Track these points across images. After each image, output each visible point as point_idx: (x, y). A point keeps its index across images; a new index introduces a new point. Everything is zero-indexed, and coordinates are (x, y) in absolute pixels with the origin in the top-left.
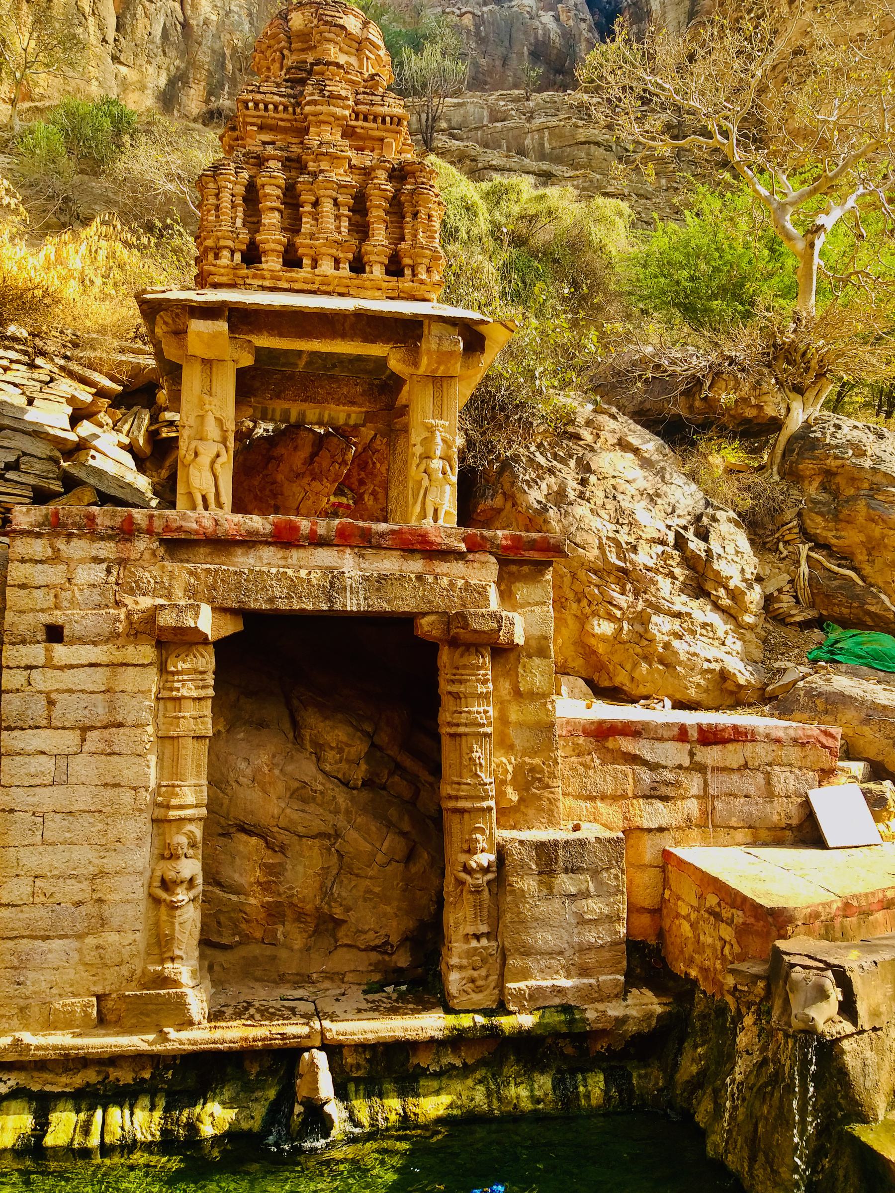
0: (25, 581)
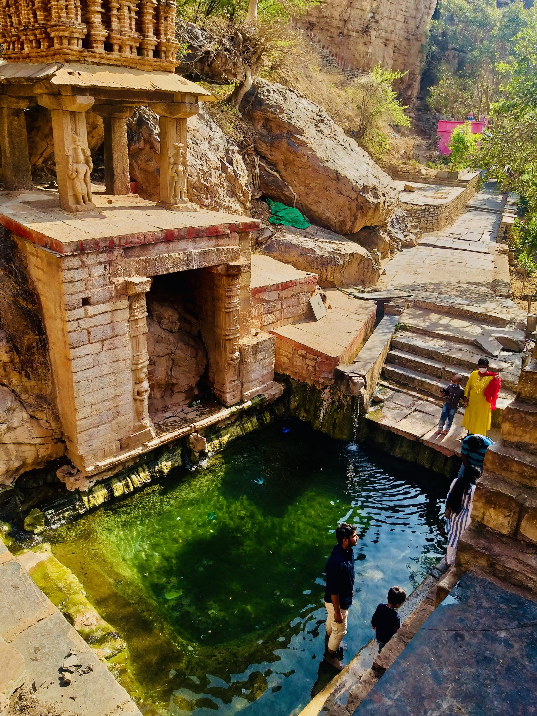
0: (71, 279)
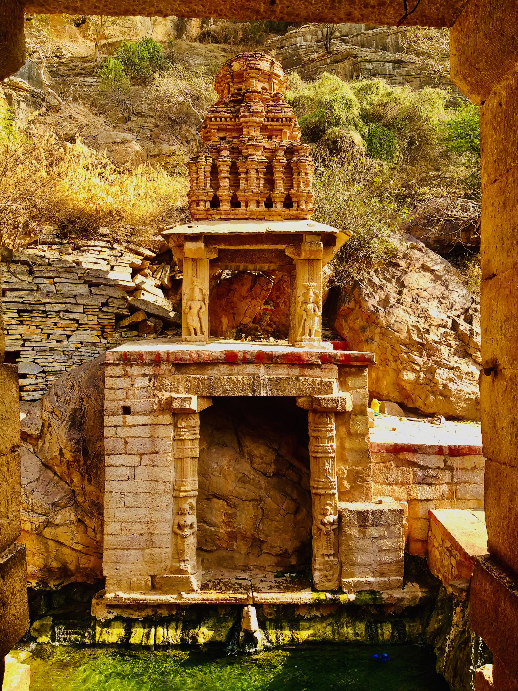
0: (112, 386)
